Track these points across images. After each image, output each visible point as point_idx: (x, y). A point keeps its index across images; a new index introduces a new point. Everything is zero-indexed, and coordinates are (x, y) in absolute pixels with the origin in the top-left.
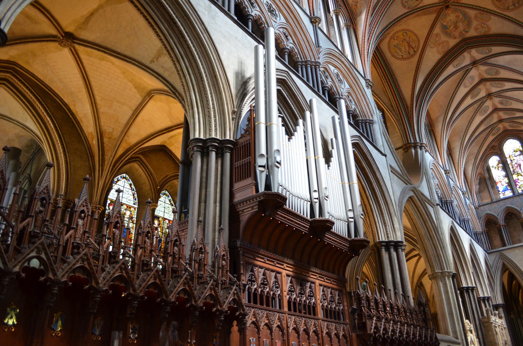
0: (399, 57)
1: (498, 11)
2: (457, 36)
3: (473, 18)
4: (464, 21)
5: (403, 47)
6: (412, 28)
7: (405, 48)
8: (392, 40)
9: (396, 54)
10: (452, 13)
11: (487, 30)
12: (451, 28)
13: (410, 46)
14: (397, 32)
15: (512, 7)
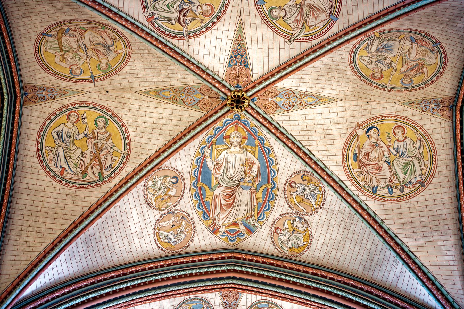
0: (54, 169)
1: (348, 183)
2: (222, 230)
3: (281, 186)
4: (257, 191)
5: (79, 151)
6: (126, 118)
7: (83, 155)
8: (63, 118)
9: (51, 155)
10: (240, 145)
11: (300, 243)
12: (218, 192)
13: (96, 156)
14: (88, 105)
15: (385, 192)
